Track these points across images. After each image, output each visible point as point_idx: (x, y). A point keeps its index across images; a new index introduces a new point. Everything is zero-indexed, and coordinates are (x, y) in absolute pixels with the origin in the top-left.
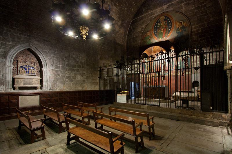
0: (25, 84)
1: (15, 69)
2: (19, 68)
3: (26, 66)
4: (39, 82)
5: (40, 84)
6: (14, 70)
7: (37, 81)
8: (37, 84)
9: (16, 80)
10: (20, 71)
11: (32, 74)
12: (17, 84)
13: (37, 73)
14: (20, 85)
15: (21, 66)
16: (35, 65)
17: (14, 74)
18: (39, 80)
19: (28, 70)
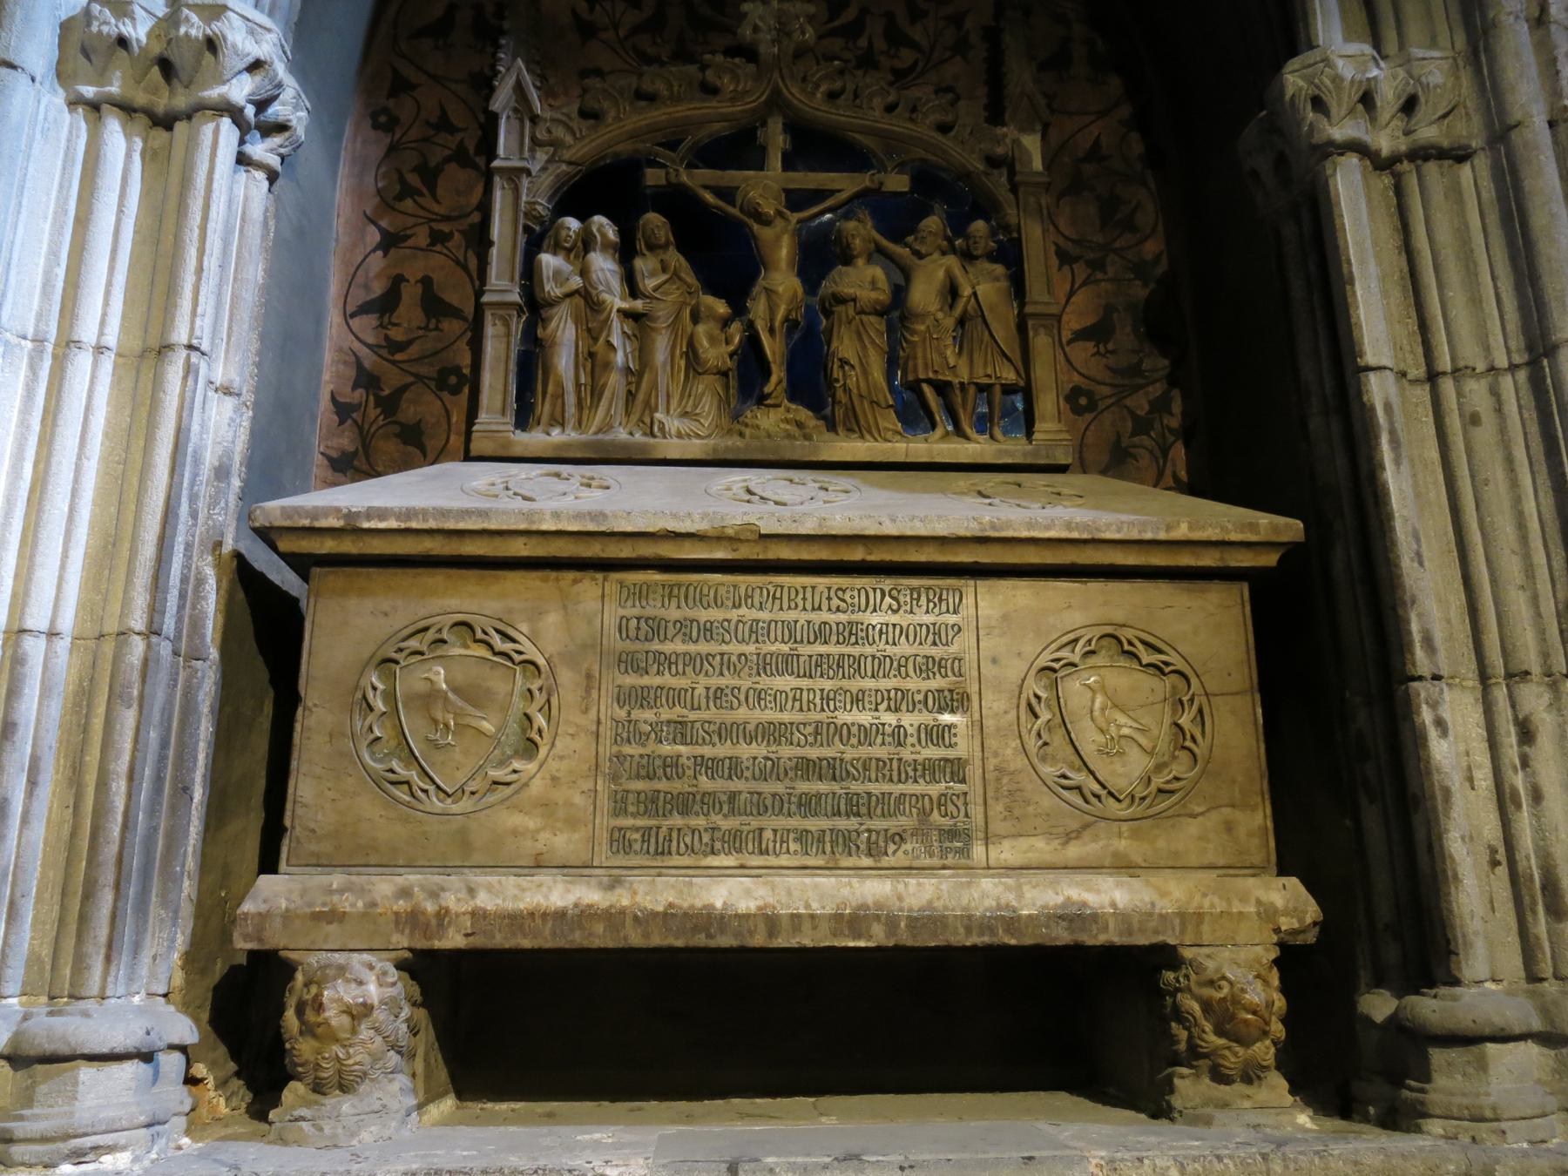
0: (659, 805)
1: (434, 307)
2: (536, 239)
3: (738, 148)
4: (1237, 731)
5: (1255, 821)
6: (409, 312)
7: (1117, 643)
8: (1159, 801)
9: (342, 631)
10: (564, 332)
11: (915, 416)
12: (370, 810)
13: (1078, 401)
14: (463, 852)
15: (584, 146)
16: (1020, 76)
17: (389, 447)
18: (1210, 632)
19: (782, 282)
